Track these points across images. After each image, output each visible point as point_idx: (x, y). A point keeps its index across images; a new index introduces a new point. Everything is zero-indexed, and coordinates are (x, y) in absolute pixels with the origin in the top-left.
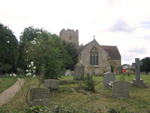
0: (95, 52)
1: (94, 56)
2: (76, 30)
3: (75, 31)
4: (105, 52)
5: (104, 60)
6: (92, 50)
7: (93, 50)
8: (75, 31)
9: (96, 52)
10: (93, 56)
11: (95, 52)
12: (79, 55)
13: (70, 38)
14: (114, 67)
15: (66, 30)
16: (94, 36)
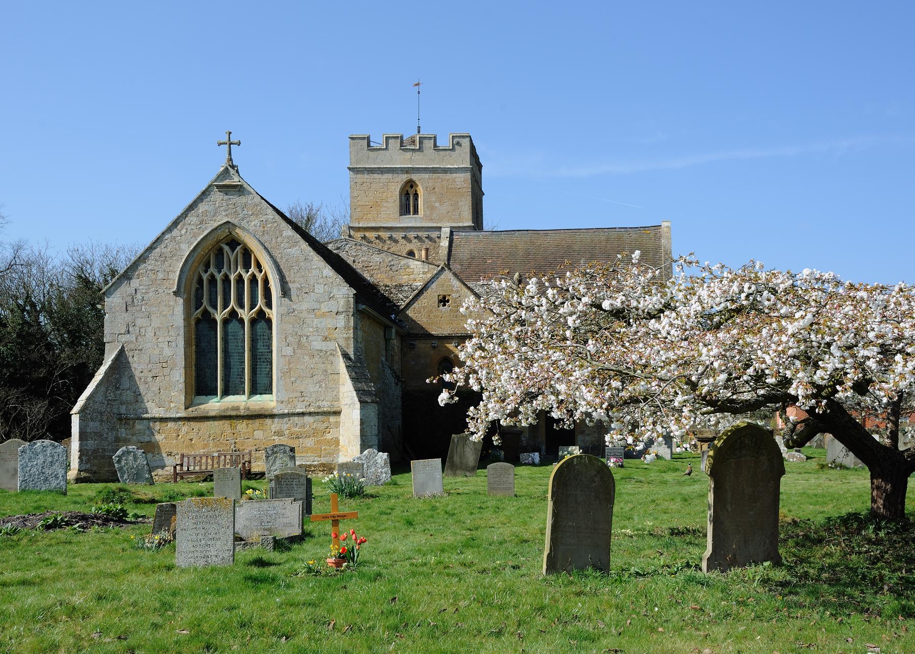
5: (317, 344)
6: (207, 266)
7: (219, 268)
11: (240, 280)
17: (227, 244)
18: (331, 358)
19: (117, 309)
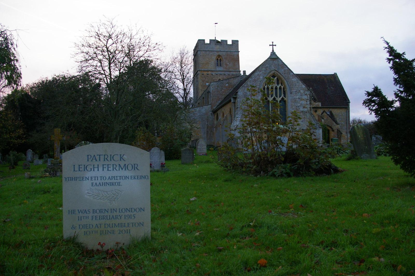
0: (276, 88)
1: (274, 99)
2: (233, 41)
3: (230, 42)
4: (304, 86)
8: (230, 42)
9: (280, 88)
10: (270, 99)
11: (276, 88)
12: (232, 99)
13: (219, 61)
14: (331, 127)
15: (207, 42)
16: (273, 45)
17: (272, 77)
18: (306, 114)
19: (242, 97)
